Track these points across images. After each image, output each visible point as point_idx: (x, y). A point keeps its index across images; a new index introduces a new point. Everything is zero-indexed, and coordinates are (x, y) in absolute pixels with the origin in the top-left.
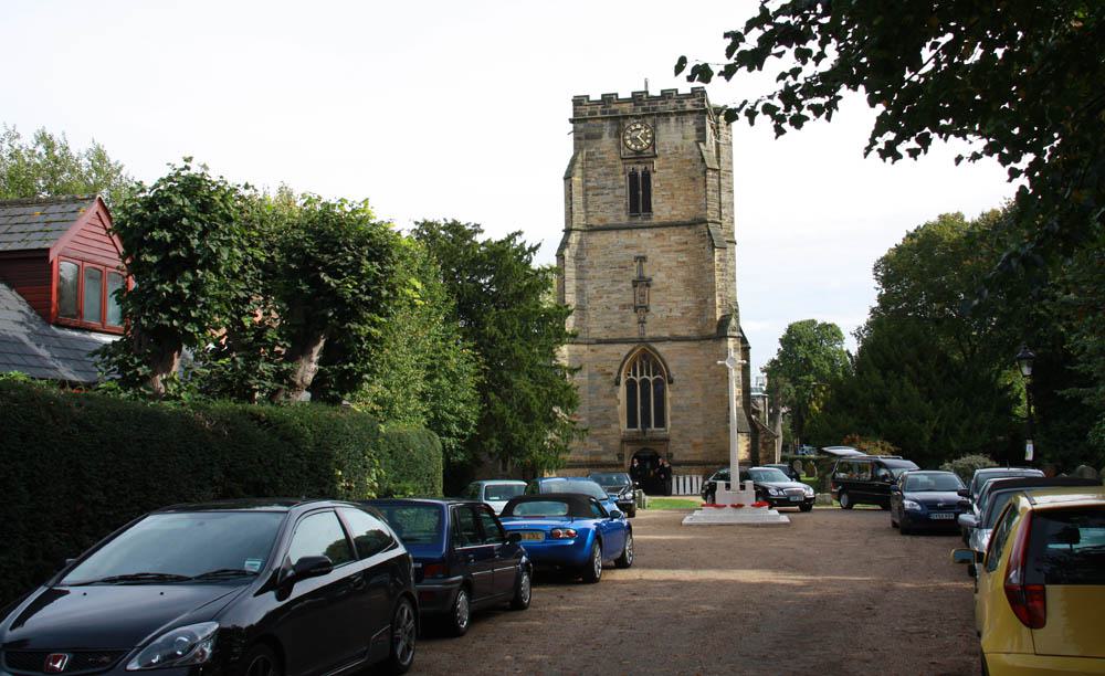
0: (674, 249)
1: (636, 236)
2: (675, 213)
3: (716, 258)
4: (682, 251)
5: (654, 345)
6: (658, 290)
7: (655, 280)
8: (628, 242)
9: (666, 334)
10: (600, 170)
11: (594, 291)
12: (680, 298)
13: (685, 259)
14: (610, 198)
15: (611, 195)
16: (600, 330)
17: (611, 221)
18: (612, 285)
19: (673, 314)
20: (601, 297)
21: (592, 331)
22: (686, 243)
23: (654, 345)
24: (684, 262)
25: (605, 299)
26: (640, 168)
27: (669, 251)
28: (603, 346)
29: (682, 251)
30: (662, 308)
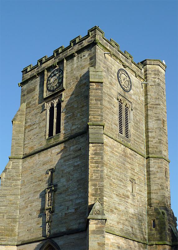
0: (72, 156)
1: (49, 153)
2: (74, 127)
3: (91, 152)
4: (76, 157)
5: (56, 240)
6: (61, 193)
7: (60, 185)
8: (46, 159)
9: (64, 230)
10: (33, 112)
11: (24, 203)
12: (75, 197)
13: (79, 163)
14: (37, 130)
15: (38, 128)
16: (24, 234)
17: (37, 147)
18: (33, 196)
19: (70, 211)
20: (27, 207)
21: (20, 236)
22: (80, 150)
23: (56, 240)
24: (78, 165)
25: (28, 209)
26: (55, 102)
27: (68, 160)
28: (26, 245)
29: (76, 157)
30: (62, 207)
